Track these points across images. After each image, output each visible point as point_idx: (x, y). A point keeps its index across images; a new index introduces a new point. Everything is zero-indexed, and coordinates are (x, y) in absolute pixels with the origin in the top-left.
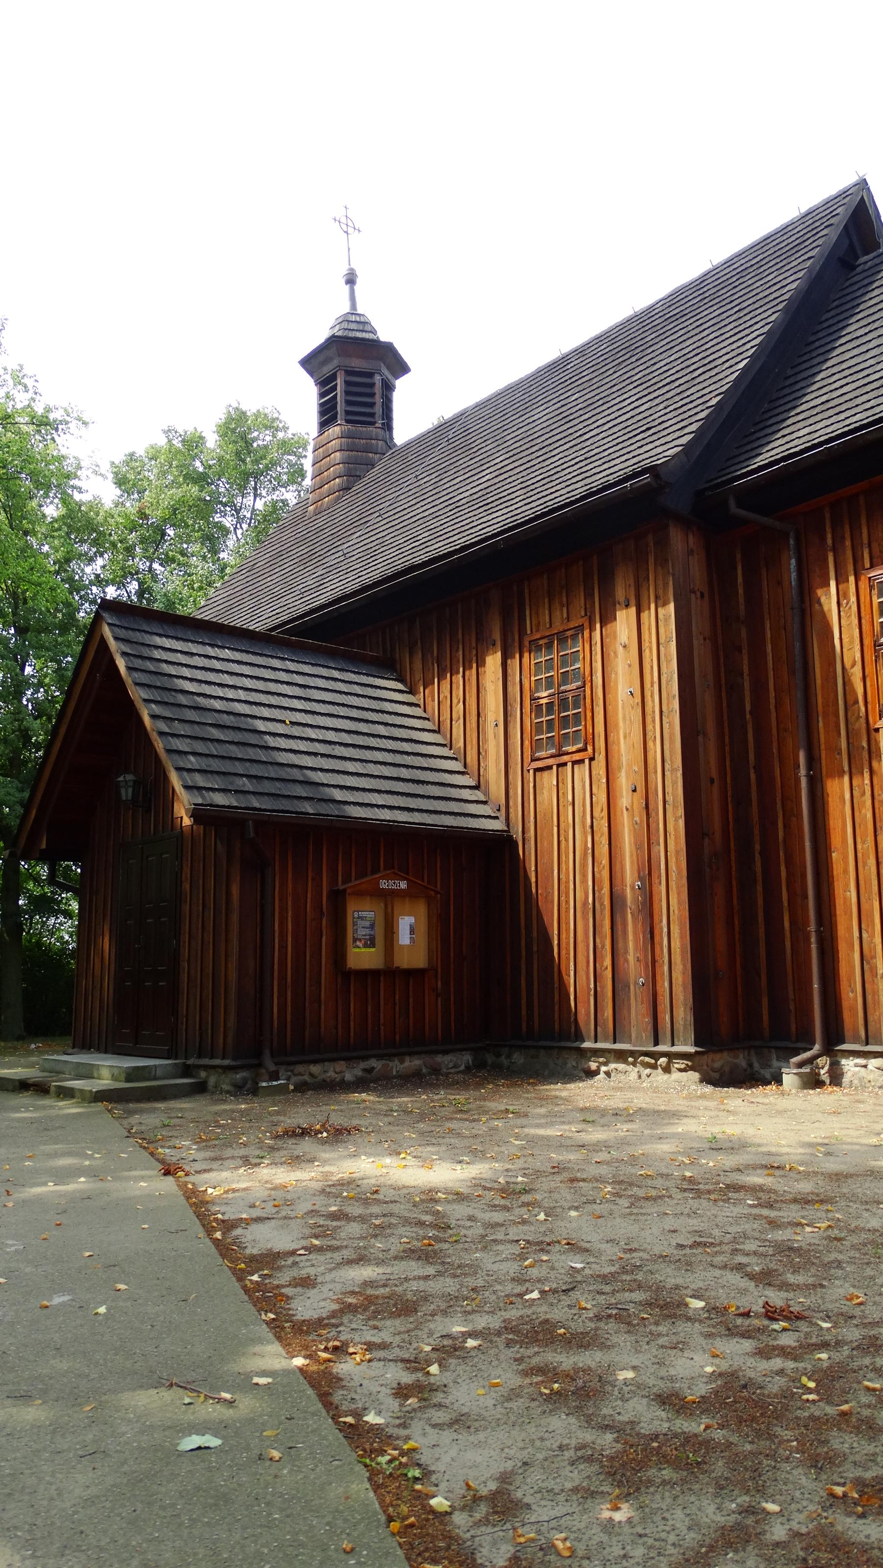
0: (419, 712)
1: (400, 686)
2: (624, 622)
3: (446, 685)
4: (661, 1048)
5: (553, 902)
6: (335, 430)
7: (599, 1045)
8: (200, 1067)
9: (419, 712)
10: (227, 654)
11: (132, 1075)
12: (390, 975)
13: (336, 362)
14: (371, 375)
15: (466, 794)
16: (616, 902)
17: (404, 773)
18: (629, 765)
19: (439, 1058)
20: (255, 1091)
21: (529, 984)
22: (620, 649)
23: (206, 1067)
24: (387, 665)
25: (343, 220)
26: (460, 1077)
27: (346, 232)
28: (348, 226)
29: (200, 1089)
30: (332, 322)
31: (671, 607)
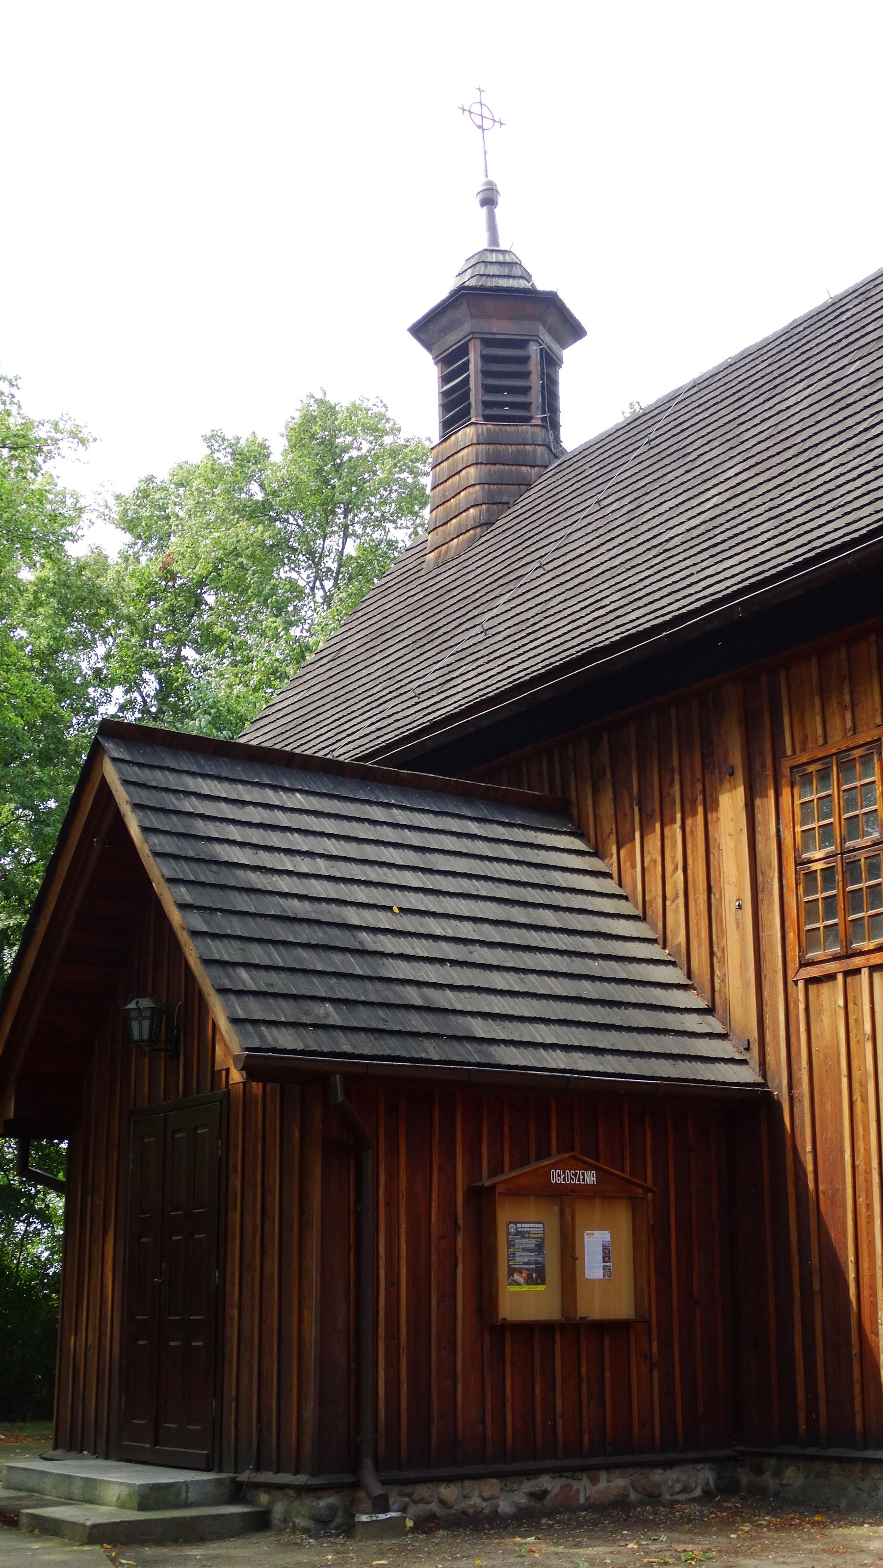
0: (610, 886)
1: (578, 844)
3: (653, 842)
5: (844, 1206)
6: (467, 433)
8: (258, 1486)
9: (610, 886)
10: (299, 800)
11: (149, 1498)
12: (572, 1333)
13: (466, 328)
14: (522, 344)
15: (692, 1022)
17: (588, 989)
19: (658, 1475)
20: (349, 1530)
23: (269, 1487)
24: (559, 811)
25: (476, 109)
26: (694, 1509)
27: (481, 127)
28: (483, 119)
29: (259, 1523)
30: (460, 265)
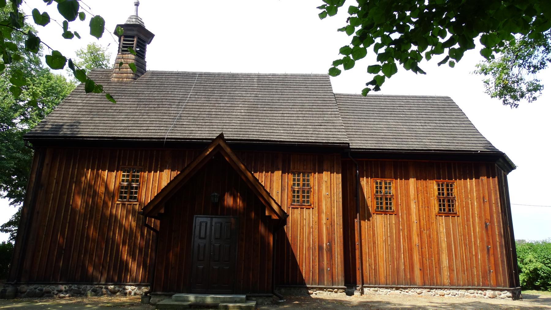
2: (326, 175)
4: (334, 287)
5: (297, 246)
13: (135, 33)
16: (320, 248)
18: (326, 213)
31: (340, 175)
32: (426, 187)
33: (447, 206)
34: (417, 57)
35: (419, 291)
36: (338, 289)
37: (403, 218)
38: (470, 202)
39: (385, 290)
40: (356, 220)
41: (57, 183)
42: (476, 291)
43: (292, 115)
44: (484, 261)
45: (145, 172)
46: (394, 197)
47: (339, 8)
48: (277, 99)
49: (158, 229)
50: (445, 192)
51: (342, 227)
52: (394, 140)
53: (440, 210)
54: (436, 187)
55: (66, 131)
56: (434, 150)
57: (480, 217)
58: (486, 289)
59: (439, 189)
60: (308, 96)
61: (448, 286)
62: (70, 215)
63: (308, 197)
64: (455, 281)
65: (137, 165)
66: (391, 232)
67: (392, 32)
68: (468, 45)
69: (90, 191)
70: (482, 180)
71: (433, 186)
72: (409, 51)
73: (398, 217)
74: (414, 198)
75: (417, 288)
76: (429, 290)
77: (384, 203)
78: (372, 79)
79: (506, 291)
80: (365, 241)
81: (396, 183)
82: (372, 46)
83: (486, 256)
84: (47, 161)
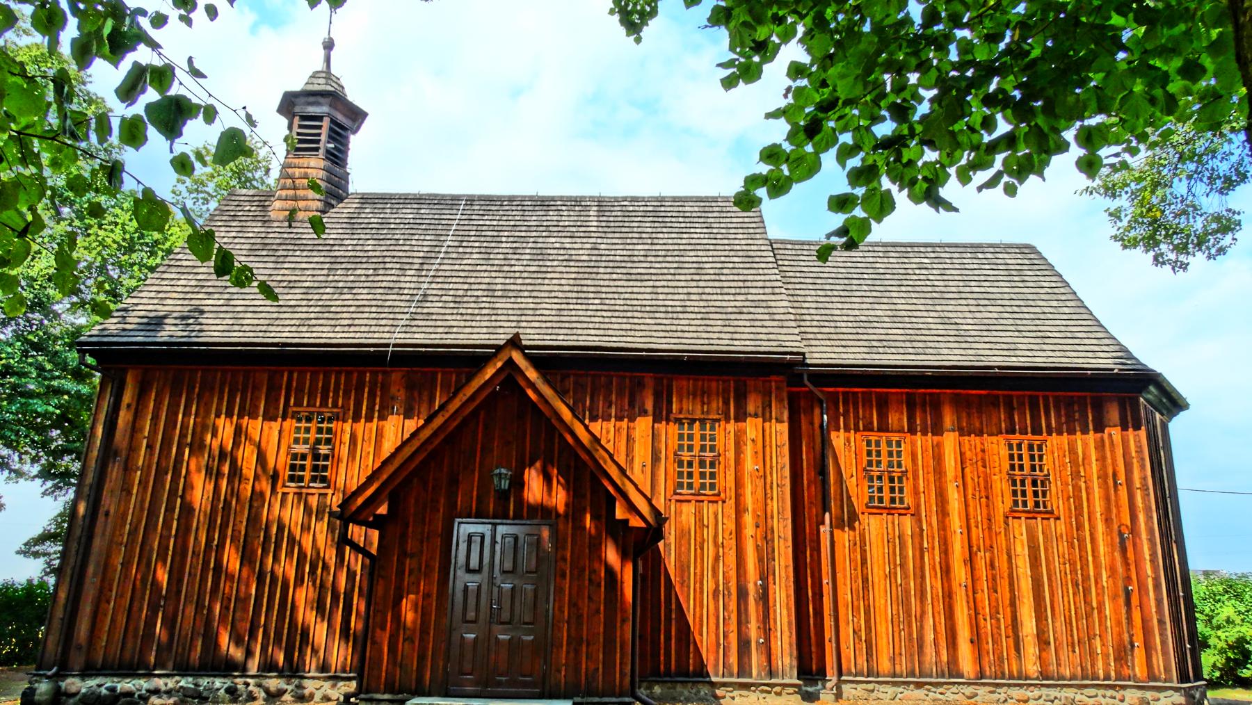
2: (752, 428)
4: (773, 681)
7: (726, 680)
13: (322, 109)
16: (742, 594)
18: (754, 511)
21: (668, 639)
22: (749, 442)
32: (983, 451)
33: (1031, 495)
34: (937, 175)
35: (969, 690)
36: (784, 686)
37: (929, 524)
38: (1083, 486)
39: (891, 690)
40: (822, 529)
41: (150, 447)
42: (1101, 692)
43: (676, 291)
44: (1119, 623)
45: (344, 421)
46: (910, 475)
47: (766, 67)
48: (642, 253)
49: (374, 551)
50: (1026, 462)
51: (790, 543)
52: (908, 344)
53: (1016, 503)
54: (1004, 452)
55: (170, 332)
56: (999, 368)
57: (1108, 521)
58: (1123, 687)
59: (1011, 457)
60: (712, 247)
61: (1037, 679)
62: (178, 520)
63: (712, 475)
64: (1053, 668)
65: (326, 406)
66: (903, 557)
67: (876, 119)
68: (1047, 145)
69: (224, 465)
70: (1110, 435)
71: (997, 447)
72: (920, 163)
73: (920, 521)
74: (956, 478)
75: (963, 684)
76: (992, 689)
77: (886, 490)
78: (840, 224)
79: (1171, 692)
80: (845, 577)
81: (913, 444)
82: (833, 152)
83: (1124, 611)
84: (127, 398)
